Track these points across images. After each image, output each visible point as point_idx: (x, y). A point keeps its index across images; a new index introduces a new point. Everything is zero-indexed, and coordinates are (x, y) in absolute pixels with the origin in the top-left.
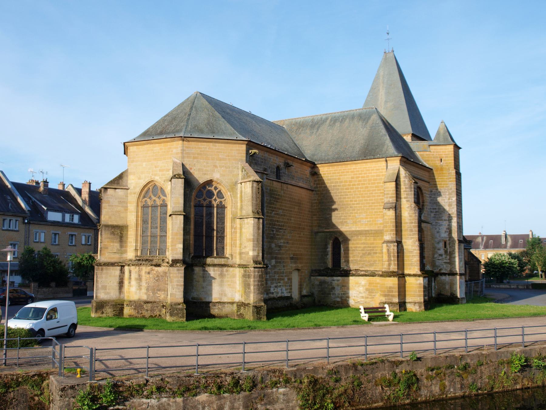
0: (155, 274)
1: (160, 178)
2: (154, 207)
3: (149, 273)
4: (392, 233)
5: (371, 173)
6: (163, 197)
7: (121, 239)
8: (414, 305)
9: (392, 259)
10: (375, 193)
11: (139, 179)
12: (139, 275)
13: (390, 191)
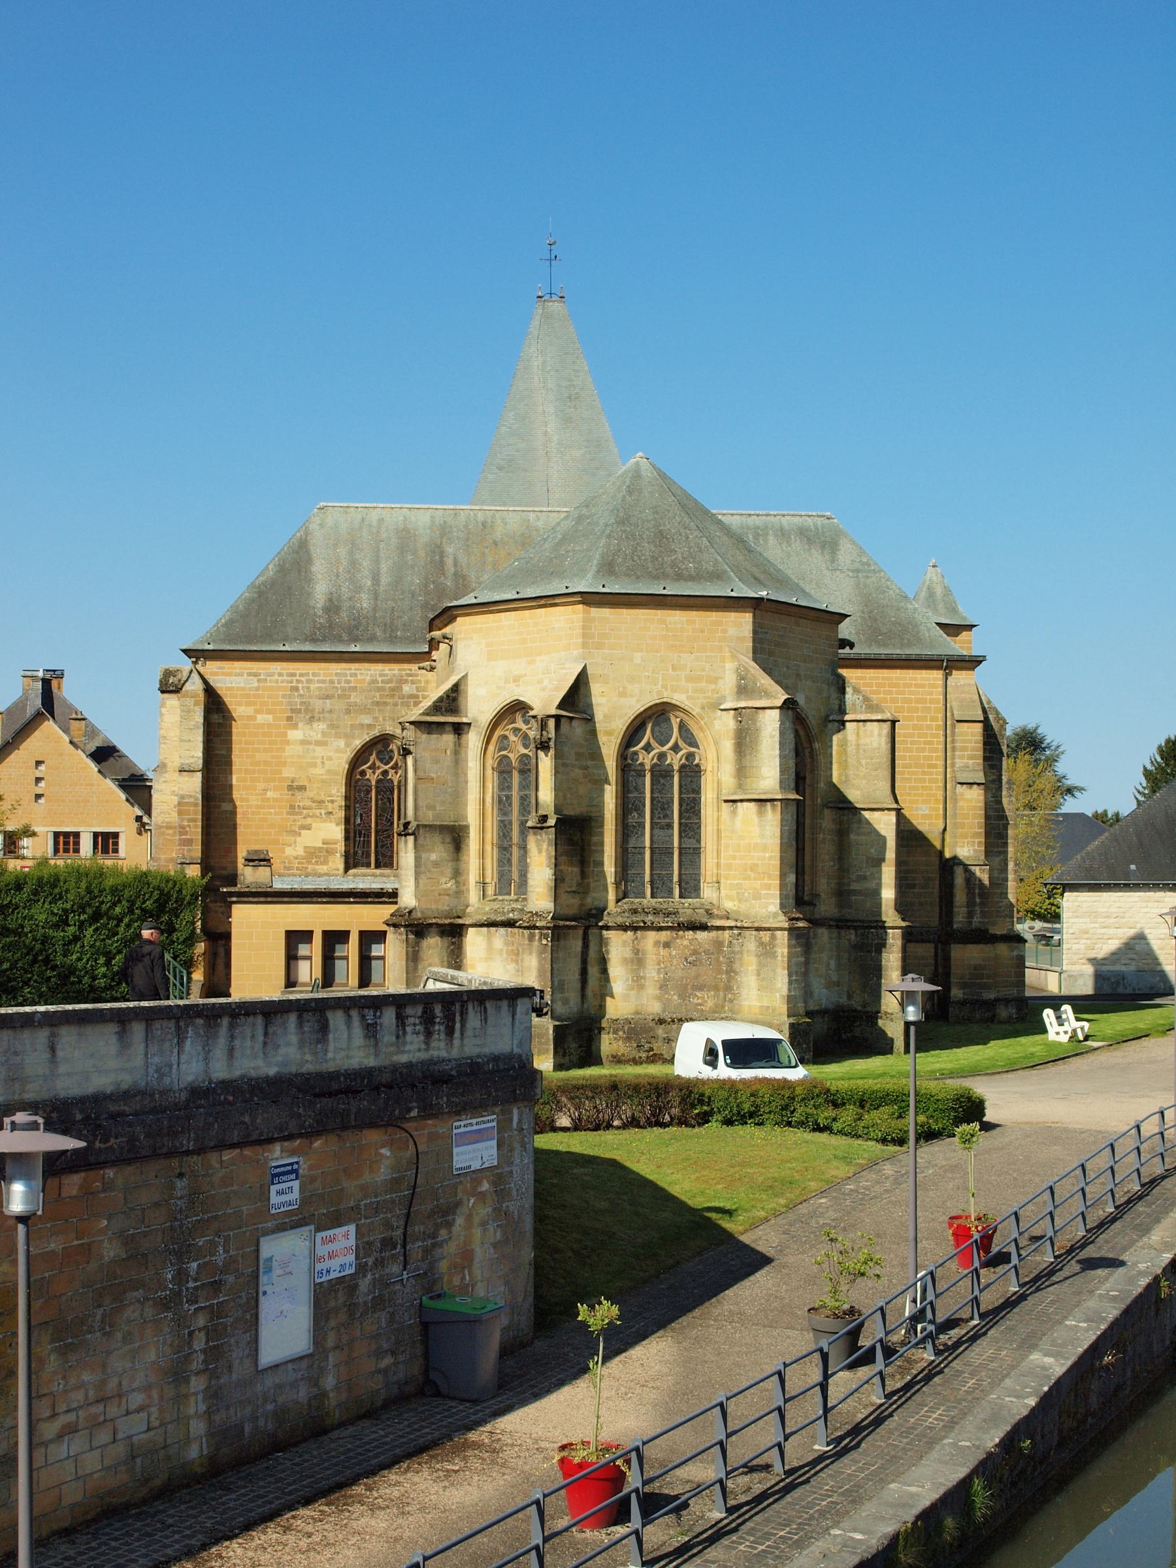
0: (686, 947)
1: (688, 698)
2: (661, 773)
3: (667, 945)
4: (977, 840)
5: (903, 693)
6: (685, 749)
7: (582, 856)
8: (1006, 1006)
9: (978, 900)
10: (912, 743)
11: (623, 694)
12: (636, 952)
13: (970, 741)
